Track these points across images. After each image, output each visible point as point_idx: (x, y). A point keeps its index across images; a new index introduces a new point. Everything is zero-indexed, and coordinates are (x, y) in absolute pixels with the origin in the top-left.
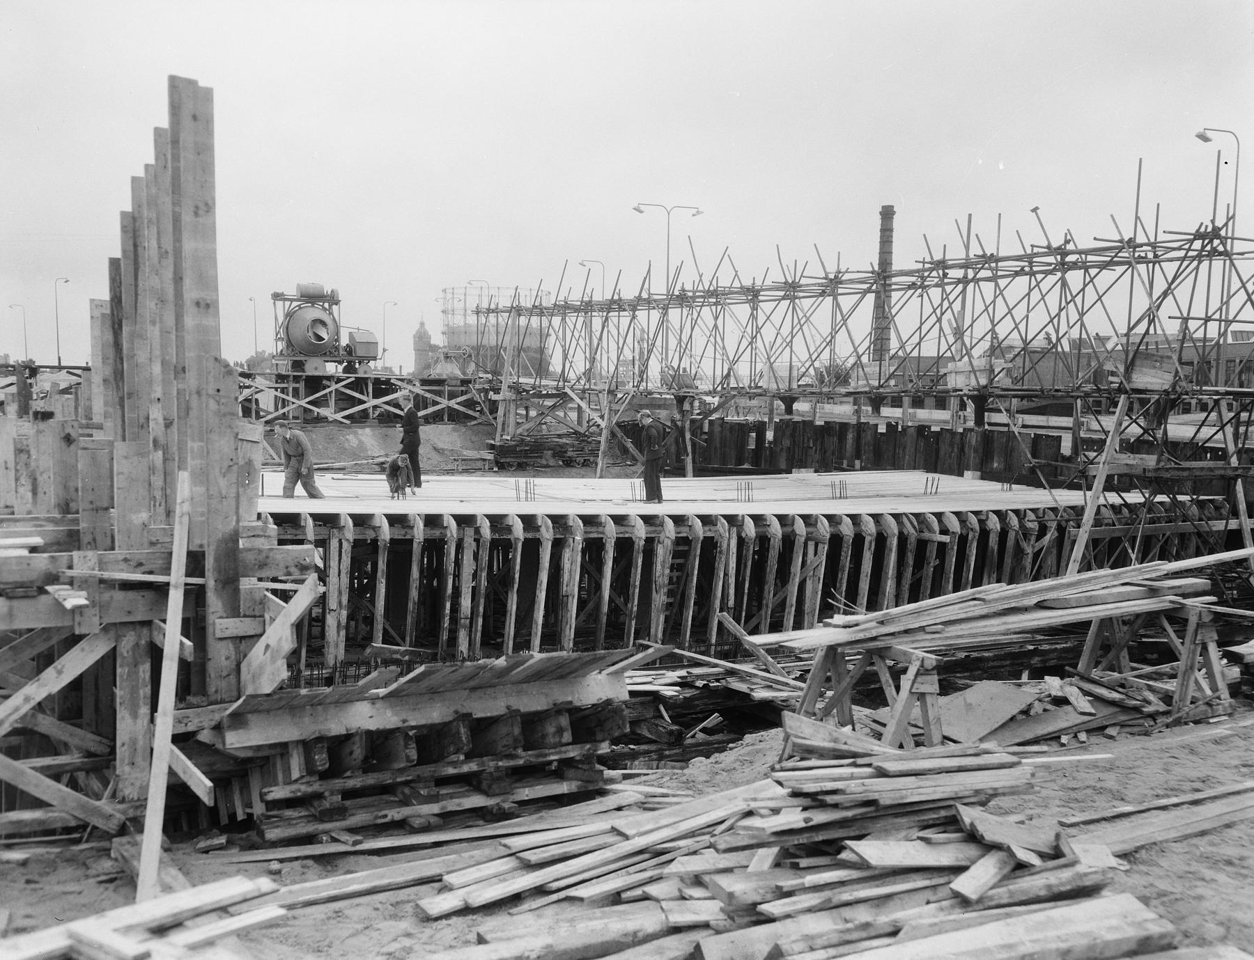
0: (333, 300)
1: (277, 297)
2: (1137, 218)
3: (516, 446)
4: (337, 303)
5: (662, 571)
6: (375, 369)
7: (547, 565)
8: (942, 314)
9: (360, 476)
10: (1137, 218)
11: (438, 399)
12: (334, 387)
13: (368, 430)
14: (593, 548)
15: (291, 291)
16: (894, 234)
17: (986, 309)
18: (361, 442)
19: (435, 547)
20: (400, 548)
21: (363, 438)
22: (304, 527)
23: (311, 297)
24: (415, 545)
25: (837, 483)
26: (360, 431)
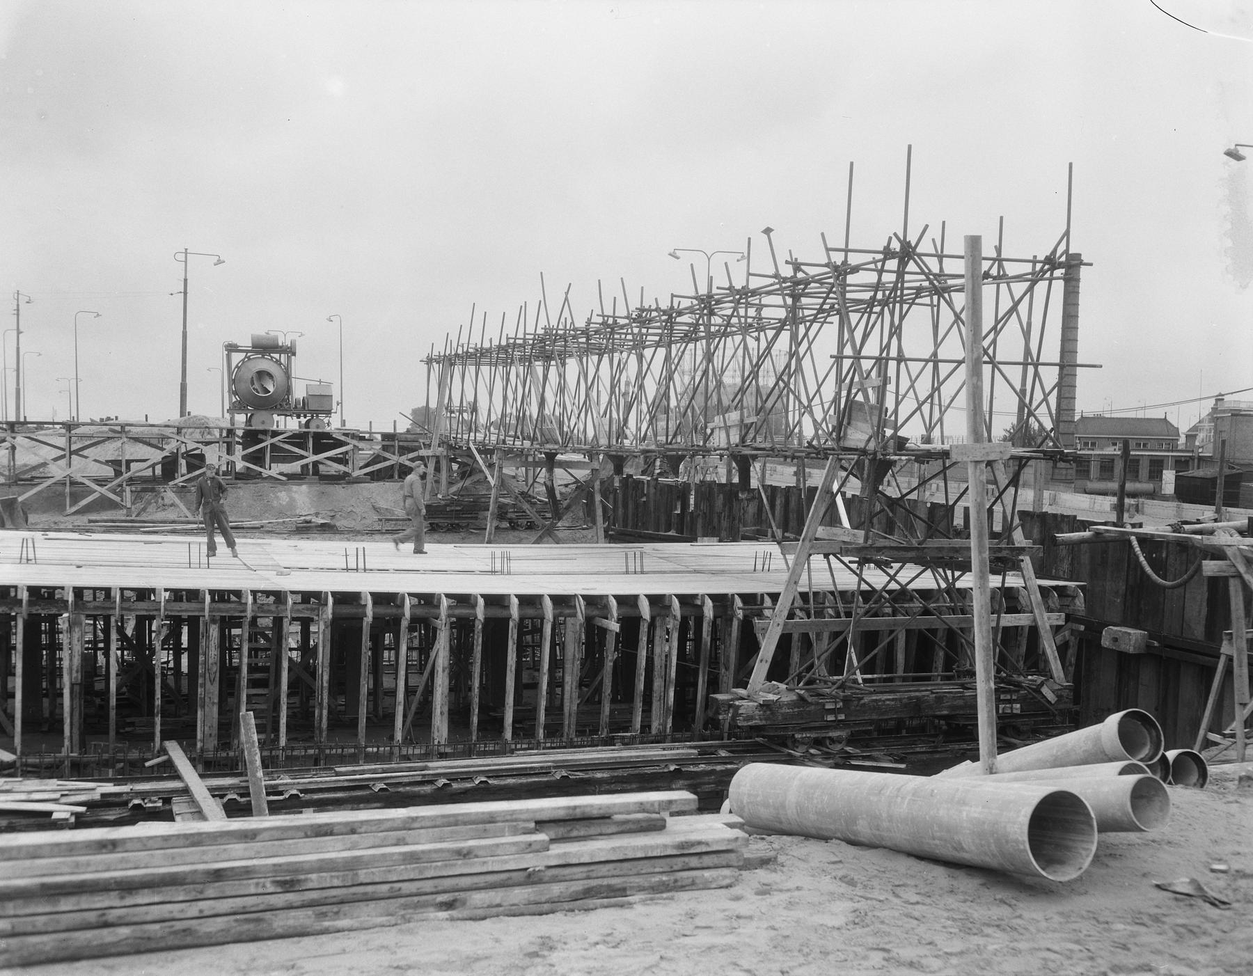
0: (290, 351)
1: (231, 348)
2: (566, 299)
3: (446, 505)
4: (294, 354)
5: (573, 652)
6: (333, 424)
7: (510, 643)
8: (777, 383)
9: (95, 536)
10: (566, 299)
11: (387, 455)
12: (269, 441)
13: (304, 487)
14: (462, 627)
15: (246, 343)
16: (1080, 308)
17: (913, 382)
18: (292, 500)
19: (531, 628)
20: (496, 628)
21: (296, 496)
22: (670, 607)
23: (265, 348)
24: (511, 624)
25: (760, 555)
26: (295, 488)
